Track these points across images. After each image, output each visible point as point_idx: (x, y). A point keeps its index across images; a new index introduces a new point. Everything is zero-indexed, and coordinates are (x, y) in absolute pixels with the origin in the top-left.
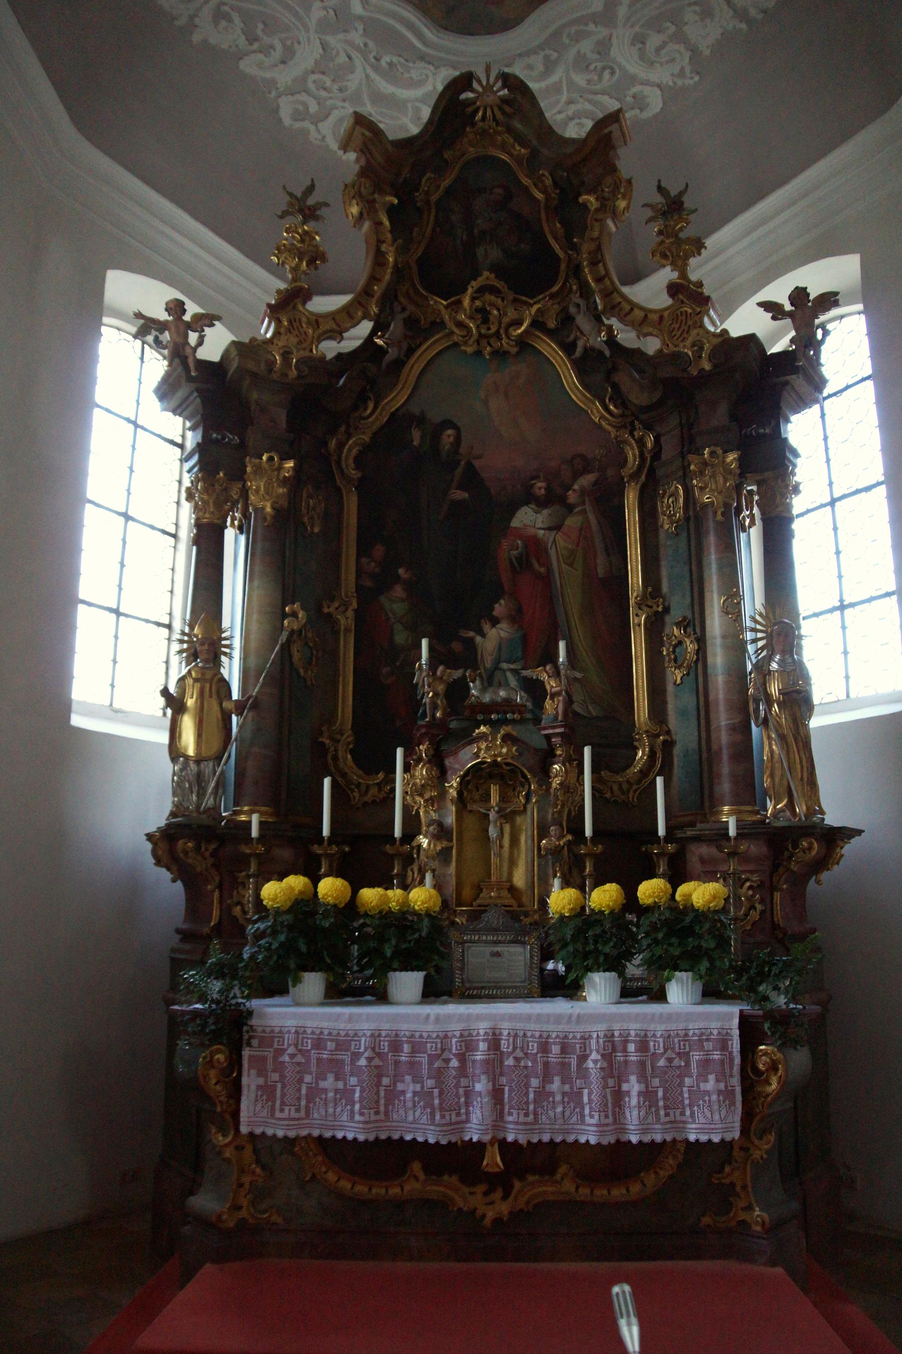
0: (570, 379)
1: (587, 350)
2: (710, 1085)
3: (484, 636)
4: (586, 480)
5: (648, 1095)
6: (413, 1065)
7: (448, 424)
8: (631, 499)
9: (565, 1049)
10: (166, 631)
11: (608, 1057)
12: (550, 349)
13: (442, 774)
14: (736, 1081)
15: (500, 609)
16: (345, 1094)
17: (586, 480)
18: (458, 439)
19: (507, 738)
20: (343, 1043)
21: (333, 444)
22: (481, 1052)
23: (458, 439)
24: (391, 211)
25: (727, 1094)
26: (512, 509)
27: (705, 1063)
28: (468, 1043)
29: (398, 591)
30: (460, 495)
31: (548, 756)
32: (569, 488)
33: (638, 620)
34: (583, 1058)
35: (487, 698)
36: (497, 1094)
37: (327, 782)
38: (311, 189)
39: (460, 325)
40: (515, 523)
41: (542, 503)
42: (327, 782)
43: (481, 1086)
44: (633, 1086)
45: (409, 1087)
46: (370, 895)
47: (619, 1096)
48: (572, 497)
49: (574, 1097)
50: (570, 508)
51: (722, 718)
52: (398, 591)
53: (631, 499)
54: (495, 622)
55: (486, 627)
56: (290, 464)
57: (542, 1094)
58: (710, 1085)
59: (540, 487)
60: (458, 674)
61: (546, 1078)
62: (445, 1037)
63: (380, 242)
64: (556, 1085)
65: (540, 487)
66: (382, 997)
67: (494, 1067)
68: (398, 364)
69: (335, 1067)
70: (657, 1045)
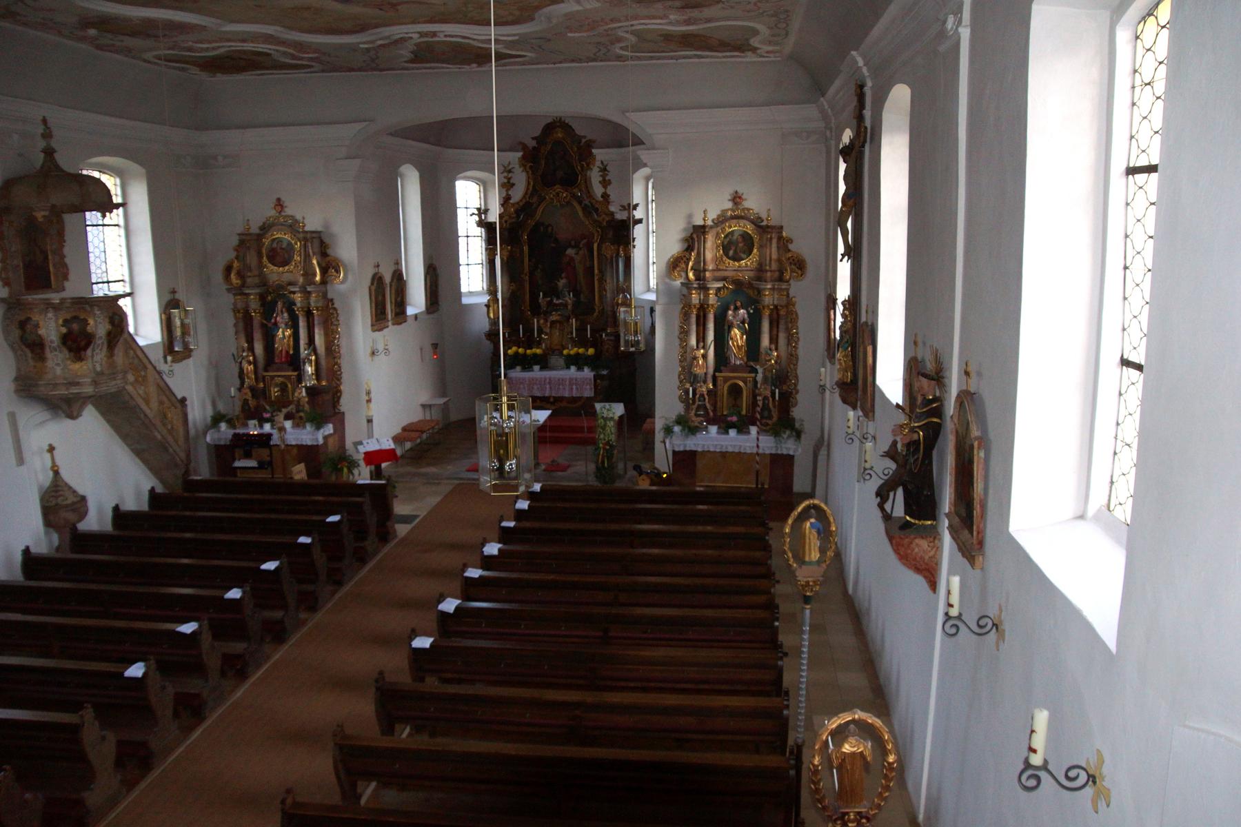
0: (580, 213)
1: (586, 205)
2: (588, 387)
3: (559, 281)
4: (585, 241)
5: (577, 389)
6: (536, 383)
7: (550, 225)
8: (595, 246)
9: (562, 380)
10: (481, 265)
11: (570, 382)
12: (575, 204)
13: (546, 321)
14: (593, 386)
15: (563, 275)
16: (524, 388)
17: (585, 241)
18: (552, 229)
19: (559, 315)
20: (524, 379)
21: (520, 232)
22: (548, 381)
23: (552, 229)
24: (531, 167)
25: (591, 389)
26: (566, 250)
27: (587, 384)
28: (545, 379)
29: (539, 270)
30: (553, 245)
31: (568, 318)
32: (580, 243)
33: (596, 278)
34: (566, 382)
35: (557, 302)
36: (551, 388)
37: (521, 326)
38: (509, 163)
39: (551, 199)
40: (567, 253)
41: (573, 247)
42: (521, 326)
43: (548, 386)
44: (574, 387)
45: (535, 387)
46: (529, 352)
47: (572, 389)
48: (581, 246)
49: (564, 389)
50: (580, 249)
51: (609, 309)
52: (539, 270)
53: (595, 246)
54: (562, 279)
55: (560, 280)
56: (509, 247)
57: (559, 388)
58: (588, 387)
59: (573, 243)
60: (549, 299)
61: (559, 385)
62: (541, 378)
63: (529, 178)
64: (561, 387)
65: (573, 243)
66: (533, 371)
67: (550, 383)
68: (537, 208)
69: (521, 383)
70: (578, 380)
